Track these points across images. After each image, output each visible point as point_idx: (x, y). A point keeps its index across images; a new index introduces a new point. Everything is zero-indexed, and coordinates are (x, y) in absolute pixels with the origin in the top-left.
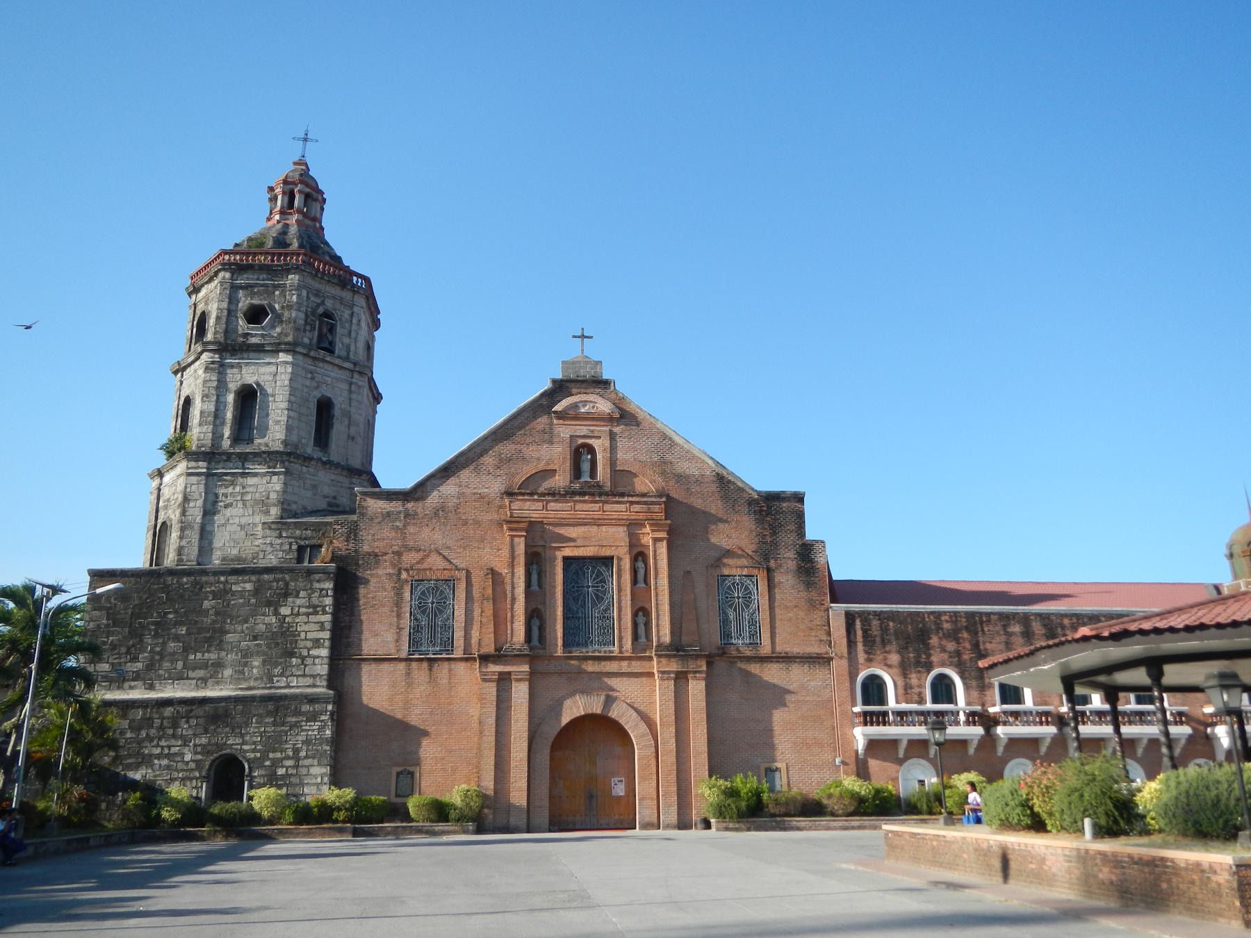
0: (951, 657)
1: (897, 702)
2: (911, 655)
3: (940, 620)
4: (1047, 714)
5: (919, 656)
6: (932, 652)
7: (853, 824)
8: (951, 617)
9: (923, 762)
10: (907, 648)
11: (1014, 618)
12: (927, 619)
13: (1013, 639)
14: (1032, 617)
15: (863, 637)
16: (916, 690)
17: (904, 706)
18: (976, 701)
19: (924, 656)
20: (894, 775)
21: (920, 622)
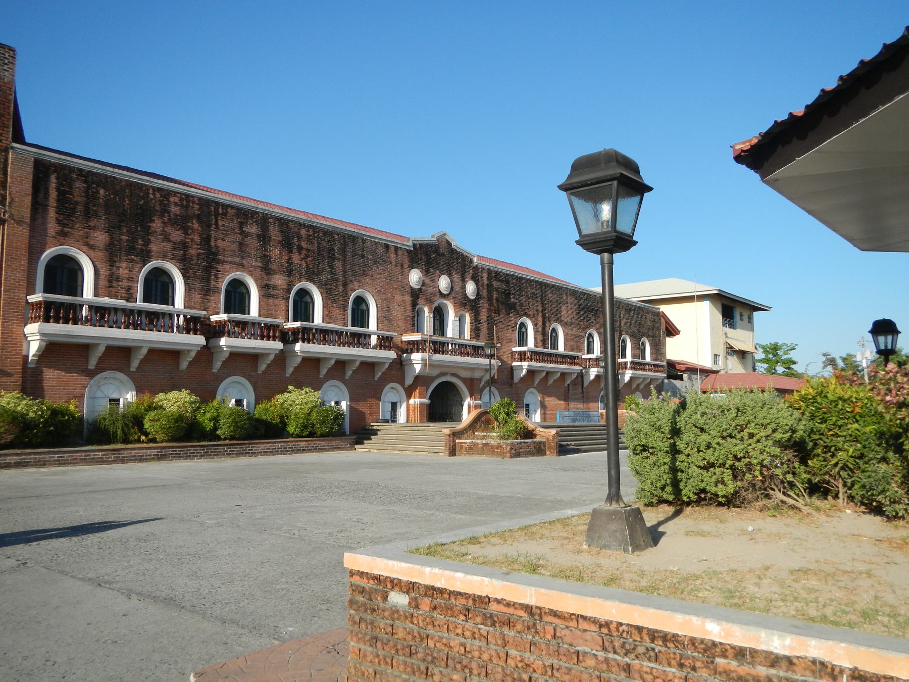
0: (175, 249)
1: (96, 294)
2: (124, 237)
3: (168, 200)
4: (275, 327)
5: (134, 241)
6: (152, 239)
7: (8, 459)
8: (181, 199)
9: (120, 375)
10: (119, 228)
11: (252, 217)
12: (151, 196)
13: (248, 240)
14: (271, 220)
15: (58, 201)
16: (125, 284)
17: (106, 301)
18: (198, 306)
19: (140, 242)
20: (78, 391)
21: (143, 198)
